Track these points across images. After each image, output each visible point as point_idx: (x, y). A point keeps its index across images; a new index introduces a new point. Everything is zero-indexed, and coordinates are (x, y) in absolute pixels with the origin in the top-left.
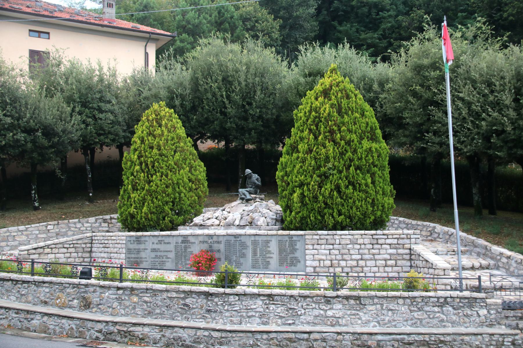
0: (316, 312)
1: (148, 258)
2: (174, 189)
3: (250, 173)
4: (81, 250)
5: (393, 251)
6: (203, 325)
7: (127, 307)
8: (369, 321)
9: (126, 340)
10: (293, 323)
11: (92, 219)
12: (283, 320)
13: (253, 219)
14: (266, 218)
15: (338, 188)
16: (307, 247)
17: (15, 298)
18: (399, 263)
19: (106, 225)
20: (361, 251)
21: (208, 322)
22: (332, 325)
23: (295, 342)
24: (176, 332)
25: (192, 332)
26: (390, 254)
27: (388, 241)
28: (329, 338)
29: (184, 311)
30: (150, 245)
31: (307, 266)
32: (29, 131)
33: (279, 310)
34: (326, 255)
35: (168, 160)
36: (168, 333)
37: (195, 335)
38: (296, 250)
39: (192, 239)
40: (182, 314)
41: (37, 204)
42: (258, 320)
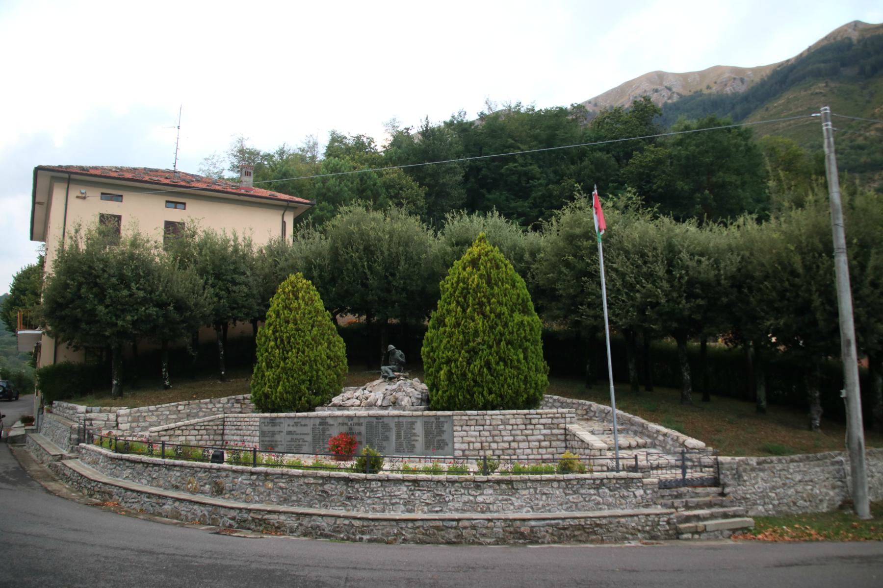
0: (465, 498)
2: (311, 367)
4: (212, 432)
5: (548, 432)
6: (343, 513)
7: (262, 493)
8: (521, 507)
9: (261, 528)
10: (441, 511)
11: (224, 400)
12: (430, 507)
13: (397, 399)
15: (488, 364)
16: (455, 428)
17: (146, 482)
18: (554, 444)
19: (239, 405)
20: (513, 432)
21: (348, 510)
22: (483, 512)
23: (442, 530)
24: (314, 521)
25: (331, 521)
26: (544, 435)
27: (542, 421)
28: (480, 525)
29: (322, 499)
30: (285, 428)
31: (455, 450)
32: (161, 305)
33: (425, 497)
34: (476, 437)
35: (305, 335)
36: (305, 521)
37: (335, 523)
38: (443, 432)
39: (330, 421)
40: (320, 502)
41: (167, 383)
42: (402, 507)
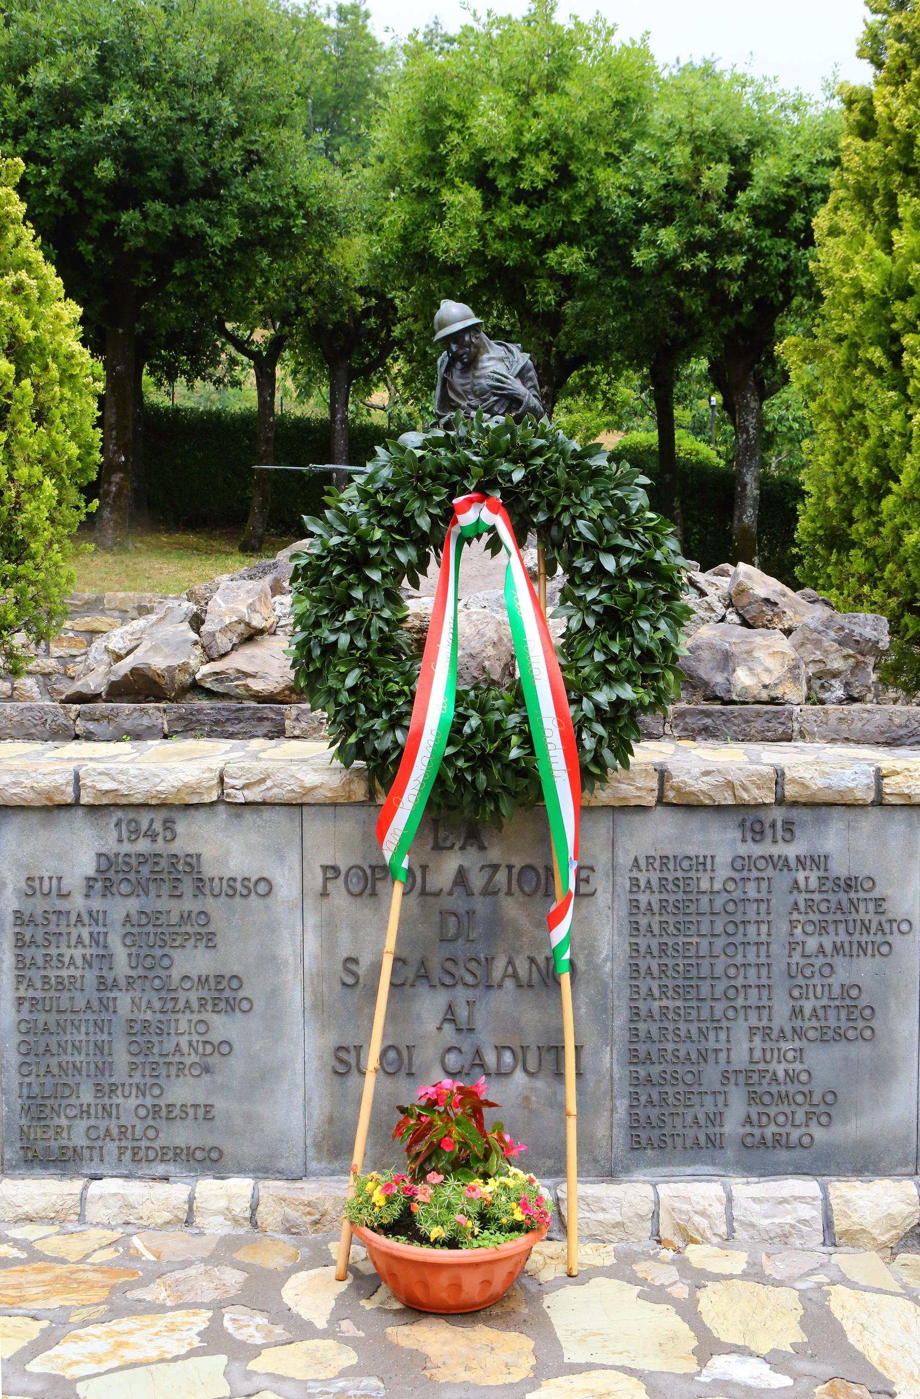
3: (474, 328)
14: (788, 632)
39: (225, 849)
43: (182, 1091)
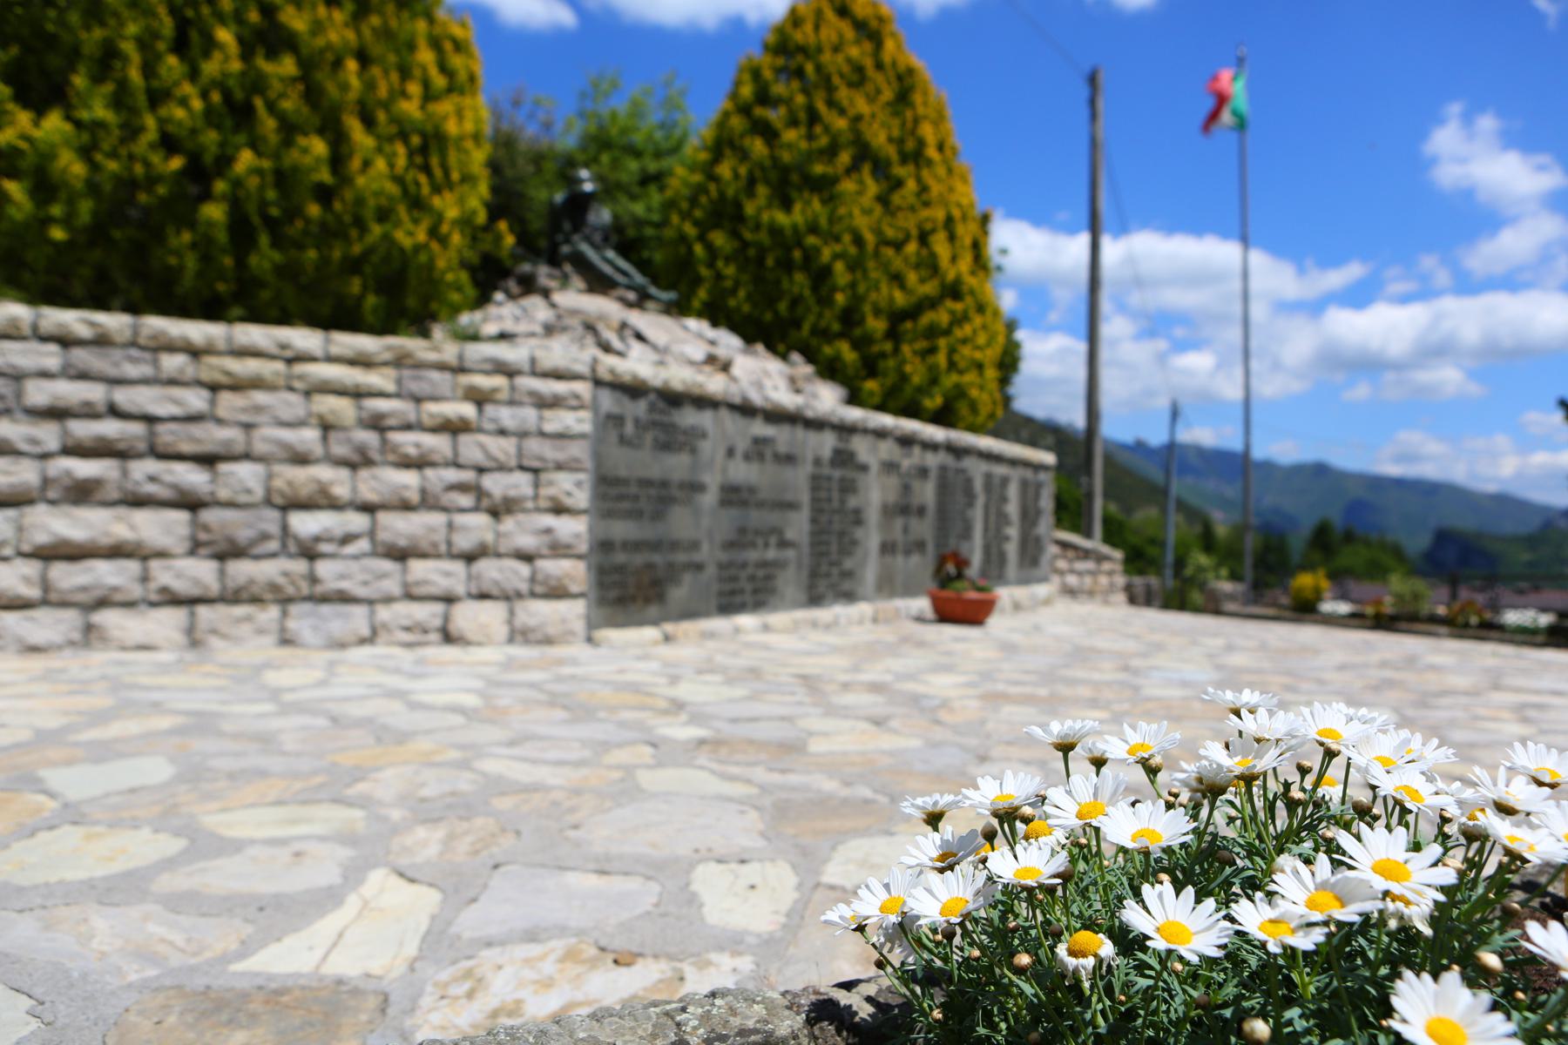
1: (705, 547)
39: (861, 447)
43: (848, 564)
